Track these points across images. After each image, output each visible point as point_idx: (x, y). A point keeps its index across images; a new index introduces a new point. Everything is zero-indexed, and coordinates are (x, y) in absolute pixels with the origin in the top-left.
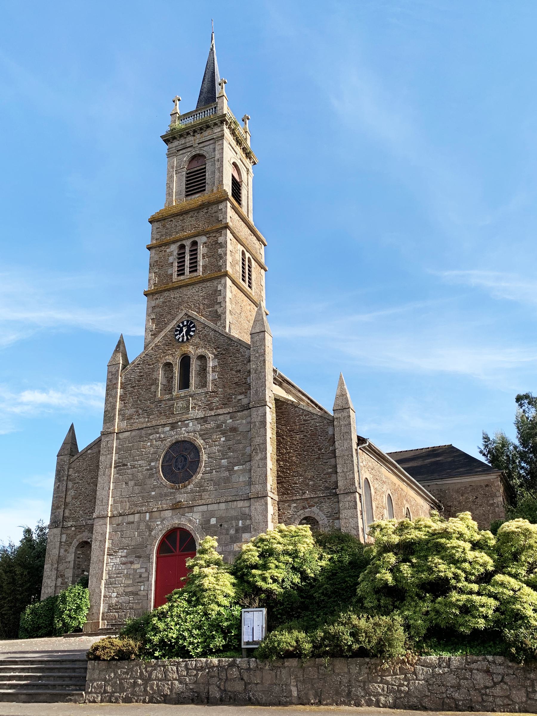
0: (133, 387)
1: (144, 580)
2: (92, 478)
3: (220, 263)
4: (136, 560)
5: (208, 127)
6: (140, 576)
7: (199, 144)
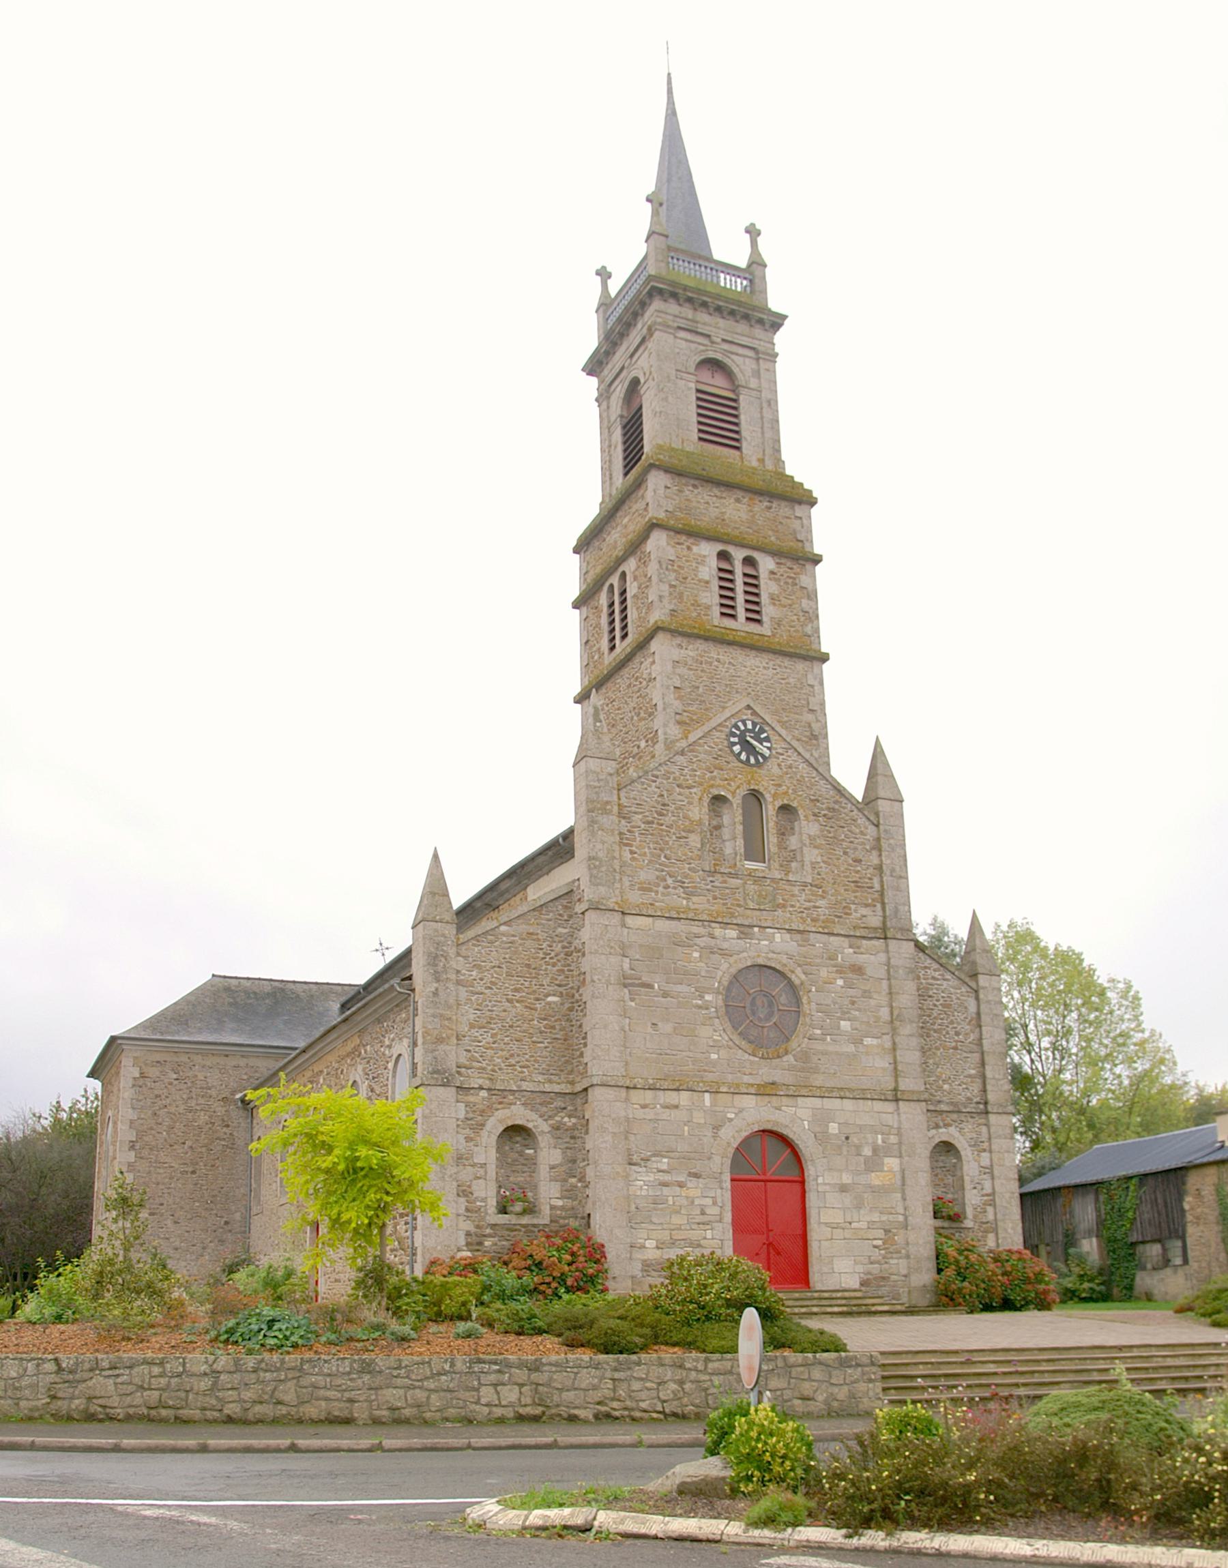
0: (649, 823)
1: (712, 1218)
2: (516, 990)
3: (808, 629)
4: (692, 1183)
5: (746, 317)
6: (703, 1213)
7: (724, 340)
